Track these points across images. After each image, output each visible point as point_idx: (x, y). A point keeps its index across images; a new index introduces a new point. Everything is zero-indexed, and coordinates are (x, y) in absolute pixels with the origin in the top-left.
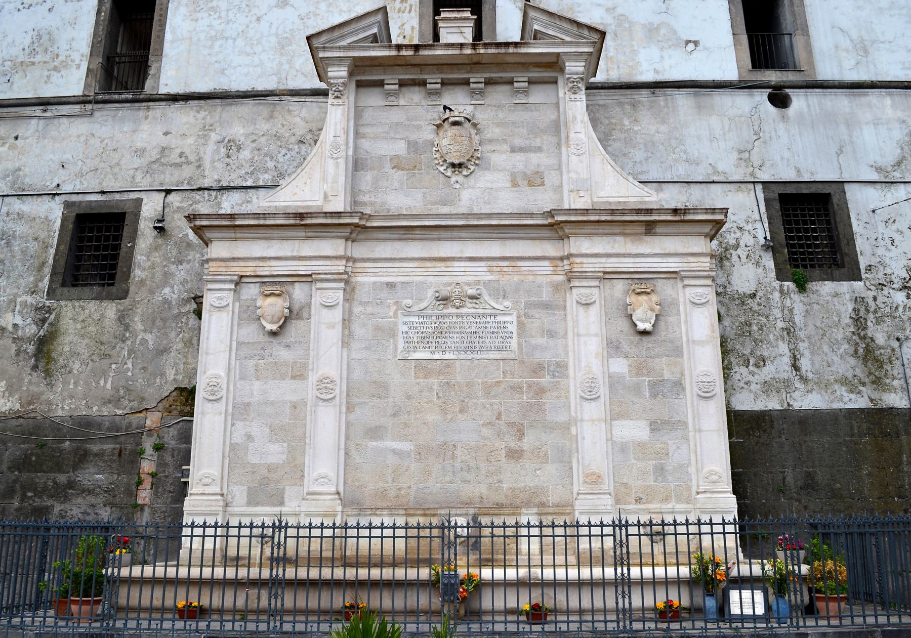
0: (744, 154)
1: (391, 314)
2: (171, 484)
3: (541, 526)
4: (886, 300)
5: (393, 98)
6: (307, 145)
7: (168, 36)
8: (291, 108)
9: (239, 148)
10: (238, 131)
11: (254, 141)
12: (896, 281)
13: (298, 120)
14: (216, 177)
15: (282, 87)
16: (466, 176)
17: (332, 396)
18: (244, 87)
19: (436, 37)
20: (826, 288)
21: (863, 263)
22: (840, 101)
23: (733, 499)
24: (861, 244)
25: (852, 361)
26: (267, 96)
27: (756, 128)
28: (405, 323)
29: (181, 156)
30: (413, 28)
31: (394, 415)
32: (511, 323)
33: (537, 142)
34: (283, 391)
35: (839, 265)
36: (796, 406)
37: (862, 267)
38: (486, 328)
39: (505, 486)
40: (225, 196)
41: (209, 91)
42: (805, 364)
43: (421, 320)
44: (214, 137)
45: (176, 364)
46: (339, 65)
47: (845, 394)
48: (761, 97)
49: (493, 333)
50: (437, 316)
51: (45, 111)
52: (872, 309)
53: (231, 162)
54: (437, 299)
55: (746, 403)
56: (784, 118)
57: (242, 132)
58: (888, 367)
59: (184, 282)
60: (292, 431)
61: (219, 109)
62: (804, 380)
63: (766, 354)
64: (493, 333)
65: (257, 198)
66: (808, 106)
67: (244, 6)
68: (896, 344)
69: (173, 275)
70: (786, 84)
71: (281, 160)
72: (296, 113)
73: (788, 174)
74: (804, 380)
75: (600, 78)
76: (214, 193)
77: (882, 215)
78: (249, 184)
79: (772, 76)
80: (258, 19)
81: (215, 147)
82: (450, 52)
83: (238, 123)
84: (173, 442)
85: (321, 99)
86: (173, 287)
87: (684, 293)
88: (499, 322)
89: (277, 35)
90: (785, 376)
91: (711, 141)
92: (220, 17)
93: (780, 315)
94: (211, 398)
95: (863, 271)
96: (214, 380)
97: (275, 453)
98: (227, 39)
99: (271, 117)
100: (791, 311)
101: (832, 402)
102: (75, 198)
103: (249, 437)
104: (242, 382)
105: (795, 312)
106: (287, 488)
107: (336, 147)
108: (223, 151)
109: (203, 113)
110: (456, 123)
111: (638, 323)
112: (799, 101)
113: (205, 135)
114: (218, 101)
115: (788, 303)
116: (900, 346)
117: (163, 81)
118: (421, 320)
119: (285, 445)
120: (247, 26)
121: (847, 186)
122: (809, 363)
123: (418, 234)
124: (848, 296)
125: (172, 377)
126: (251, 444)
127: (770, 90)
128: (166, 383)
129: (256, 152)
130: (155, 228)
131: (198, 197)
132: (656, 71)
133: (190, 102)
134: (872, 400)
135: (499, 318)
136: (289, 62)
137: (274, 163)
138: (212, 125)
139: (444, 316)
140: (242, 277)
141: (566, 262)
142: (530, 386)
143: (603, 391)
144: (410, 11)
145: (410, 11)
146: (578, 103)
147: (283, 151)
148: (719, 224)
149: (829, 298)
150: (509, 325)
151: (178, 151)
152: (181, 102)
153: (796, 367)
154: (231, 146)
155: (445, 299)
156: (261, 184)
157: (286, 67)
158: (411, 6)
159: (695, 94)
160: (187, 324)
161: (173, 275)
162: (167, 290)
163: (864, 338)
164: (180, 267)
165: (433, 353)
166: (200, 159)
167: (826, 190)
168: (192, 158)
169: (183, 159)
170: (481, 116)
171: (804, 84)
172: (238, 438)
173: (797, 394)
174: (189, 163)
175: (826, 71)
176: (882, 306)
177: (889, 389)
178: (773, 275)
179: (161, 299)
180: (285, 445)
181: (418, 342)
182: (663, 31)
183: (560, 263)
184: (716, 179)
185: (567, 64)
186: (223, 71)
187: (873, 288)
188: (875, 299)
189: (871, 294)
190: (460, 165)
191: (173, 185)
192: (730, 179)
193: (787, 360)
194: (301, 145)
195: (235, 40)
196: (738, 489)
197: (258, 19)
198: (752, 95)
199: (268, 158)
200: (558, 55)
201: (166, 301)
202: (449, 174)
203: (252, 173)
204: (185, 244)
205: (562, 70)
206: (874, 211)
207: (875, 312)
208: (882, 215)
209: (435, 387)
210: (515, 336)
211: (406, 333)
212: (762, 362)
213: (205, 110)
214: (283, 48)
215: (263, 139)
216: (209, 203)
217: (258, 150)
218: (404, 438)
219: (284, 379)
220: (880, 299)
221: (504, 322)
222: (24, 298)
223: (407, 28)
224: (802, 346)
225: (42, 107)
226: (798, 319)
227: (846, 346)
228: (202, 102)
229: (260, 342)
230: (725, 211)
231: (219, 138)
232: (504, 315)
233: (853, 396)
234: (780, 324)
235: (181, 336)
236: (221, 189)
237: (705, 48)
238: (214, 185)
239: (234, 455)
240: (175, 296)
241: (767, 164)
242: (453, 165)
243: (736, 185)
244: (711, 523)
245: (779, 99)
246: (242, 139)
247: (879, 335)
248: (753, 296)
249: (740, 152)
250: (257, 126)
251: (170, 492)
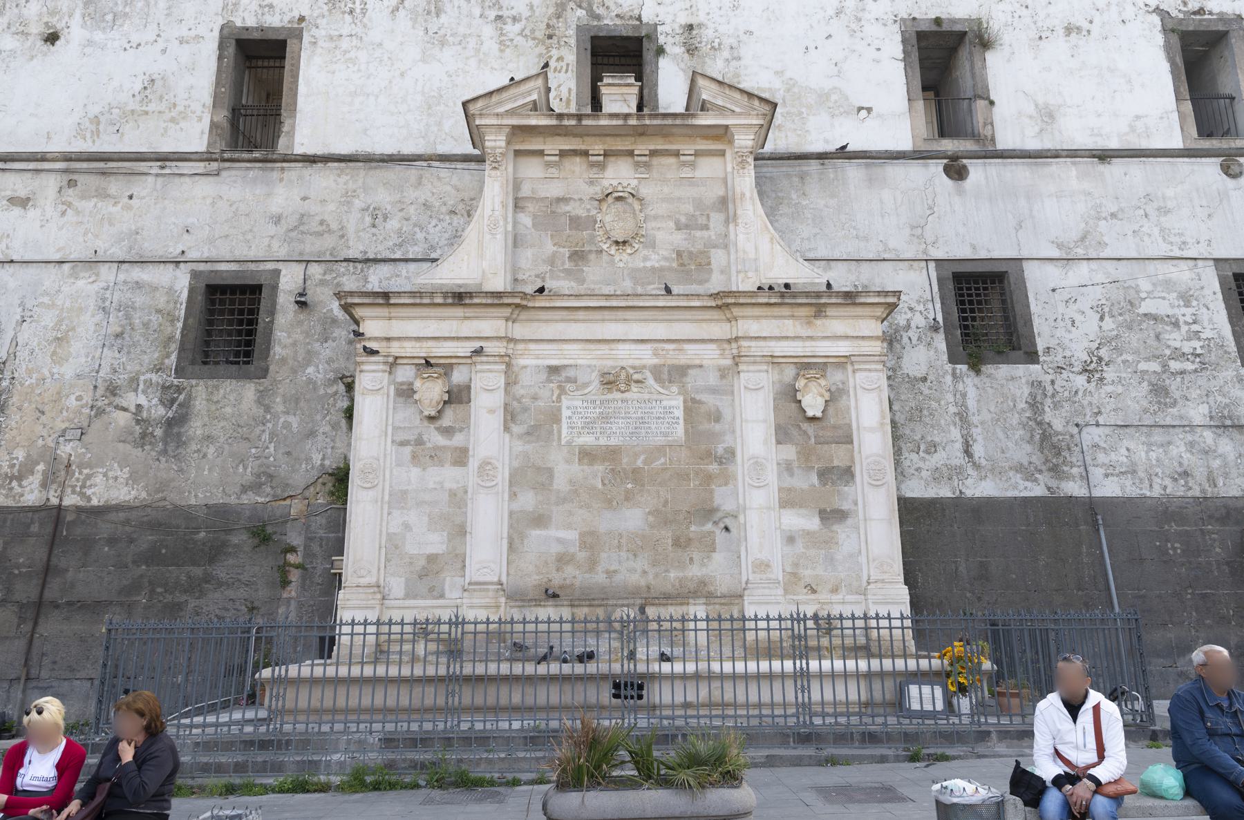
0: (917, 230)
3: (708, 620)
4: (1065, 383)
5: (553, 170)
7: (302, 89)
8: (442, 175)
9: (385, 218)
10: (383, 198)
14: (361, 248)
18: (389, 149)
19: (596, 104)
20: (1003, 371)
21: (1041, 345)
22: (1018, 172)
23: (904, 592)
25: (1028, 448)
27: (930, 202)
29: (322, 223)
30: (570, 90)
32: (677, 408)
36: (969, 493)
40: (371, 270)
42: (978, 450)
44: (358, 204)
48: (937, 167)
50: (602, 402)
51: (162, 168)
52: (1049, 394)
55: (917, 489)
56: (960, 193)
59: (329, 361)
61: (362, 173)
62: (977, 466)
63: (937, 439)
66: (986, 178)
67: (385, 58)
68: (1076, 430)
71: (432, 231)
74: (977, 466)
75: (769, 148)
76: (359, 266)
78: (397, 256)
79: (948, 145)
80: (402, 75)
82: (614, 122)
83: (379, 189)
85: (473, 165)
90: (957, 462)
91: (883, 216)
92: (359, 70)
93: (952, 400)
97: (436, 543)
100: (964, 395)
101: (1006, 490)
102: (202, 267)
103: (407, 527)
108: (368, 220)
109: (344, 178)
110: (619, 199)
112: (977, 171)
115: (960, 387)
117: (298, 138)
121: (1025, 264)
122: (982, 450)
124: (1023, 380)
127: (945, 161)
130: (297, 302)
132: (826, 141)
134: (1049, 489)
136: (439, 124)
140: (397, 358)
141: (734, 345)
142: (697, 474)
144: (567, 71)
145: (567, 71)
147: (434, 222)
148: (892, 307)
149: (1004, 382)
151: (318, 218)
152: (320, 165)
153: (968, 452)
154: (377, 216)
157: (435, 129)
159: (867, 165)
160: (334, 405)
162: (310, 370)
163: (1040, 424)
164: (325, 345)
168: (334, 226)
170: (644, 191)
172: (395, 527)
173: (969, 482)
175: (1005, 140)
176: (1058, 389)
177: (1069, 477)
178: (945, 357)
182: (834, 97)
184: (887, 256)
186: (365, 131)
187: (1050, 371)
188: (1053, 382)
190: (624, 242)
192: (902, 257)
193: (959, 445)
195: (377, 97)
196: (909, 580)
197: (402, 75)
198: (926, 165)
199: (417, 229)
200: (727, 127)
201: (310, 381)
202: (612, 252)
203: (401, 245)
205: (731, 142)
206: (1054, 290)
207: (1053, 396)
210: (681, 421)
212: (933, 448)
214: (430, 108)
215: (412, 210)
217: (407, 220)
218: (569, 527)
220: (1059, 383)
222: (148, 376)
224: (975, 432)
225: (159, 163)
226: (971, 403)
227: (1021, 432)
228: (343, 165)
230: (897, 294)
231: (363, 205)
233: (1028, 484)
234: (952, 409)
236: (367, 261)
238: (360, 256)
239: (392, 546)
242: (617, 243)
244: (889, 618)
245: (956, 171)
246: (389, 207)
247: (1057, 421)
248: (924, 379)
249: (913, 228)
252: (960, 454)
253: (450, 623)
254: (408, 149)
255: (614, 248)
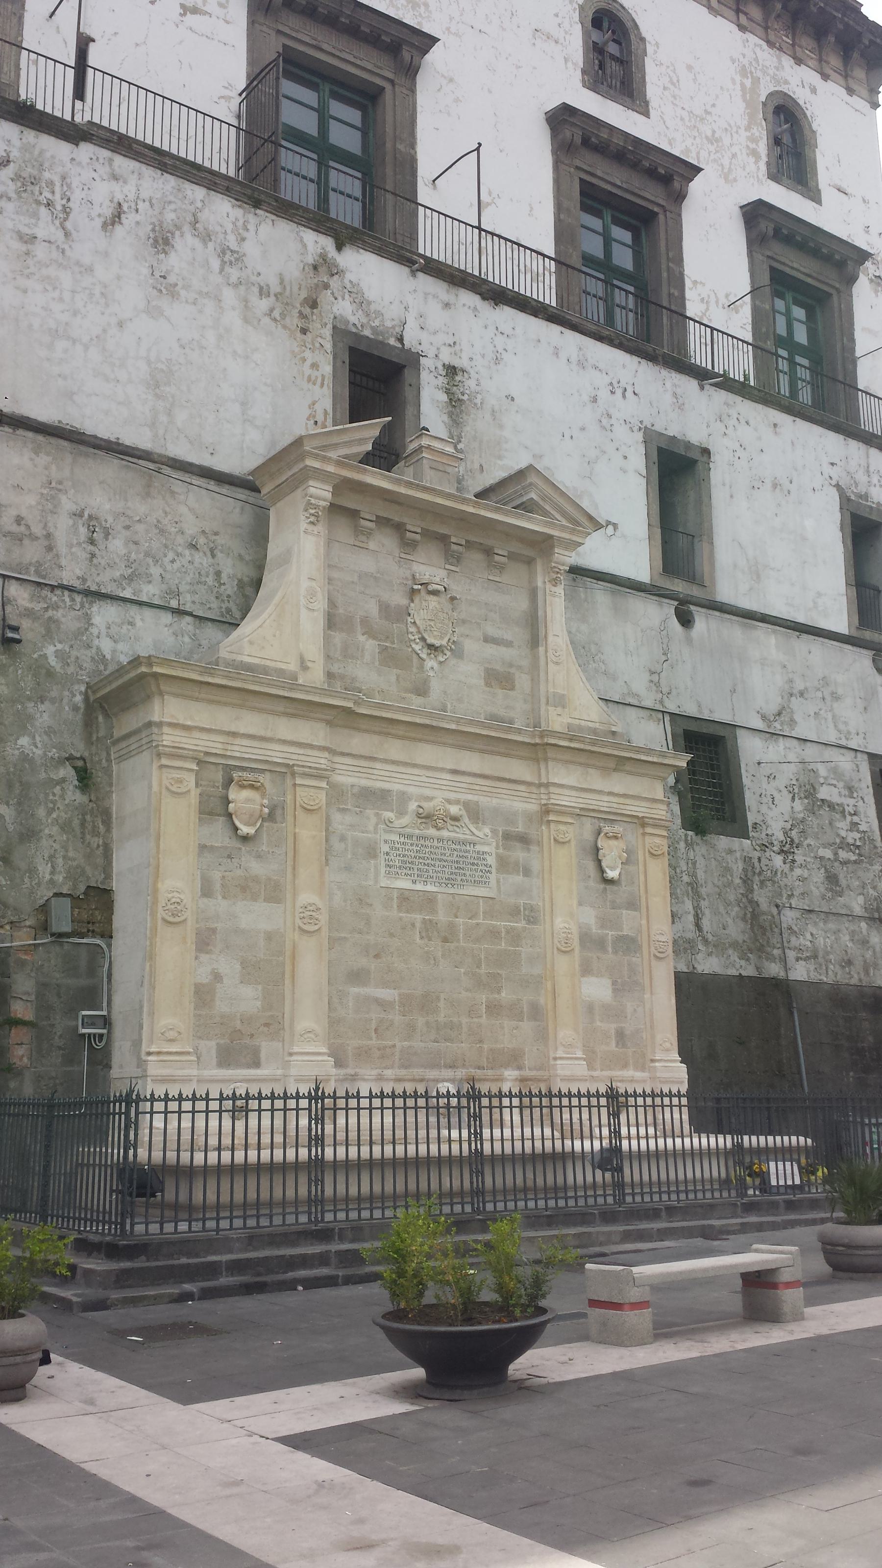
1: (371, 828)
2: (61, 1036)
4: (768, 862)
5: (364, 538)
6: (201, 554)
8: (174, 488)
9: (107, 535)
10: (101, 503)
11: (127, 528)
12: (775, 843)
13: (183, 509)
14: (79, 573)
15: (159, 450)
16: (441, 663)
17: (316, 927)
18: (104, 432)
20: (723, 842)
21: (751, 818)
22: (733, 631)
24: (750, 800)
25: (741, 925)
26: (139, 458)
27: (665, 646)
28: (386, 842)
29: (19, 520)
31: (377, 956)
32: (490, 854)
33: (508, 636)
34: (254, 917)
35: (733, 820)
36: (700, 969)
37: (750, 824)
38: (466, 857)
39: (485, 1046)
40: (95, 608)
41: (50, 422)
42: (706, 923)
43: (402, 840)
44: (67, 504)
45: (52, 857)
46: (323, 481)
47: (737, 960)
48: (669, 609)
49: (473, 864)
50: (419, 838)
52: (757, 871)
53: (97, 551)
54: (419, 816)
57: (107, 506)
58: (768, 934)
59: (49, 731)
60: (270, 969)
61: (69, 458)
62: (706, 941)
64: (473, 864)
65: (142, 620)
66: (708, 630)
67: (97, 291)
68: (775, 911)
69: (30, 718)
70: (694, 599)
71: (169, 567)
72: (182, 497)
73: (691, 710)
74: (706, 941)
76: (78, 598)
77: (766, 770)
78: (127, 594)
79: (679, 586)
80: (121, 325)
81: (71, 522)
83: (101, 490)
84: (58, 975)
86: (34, 738)
87: (644, 841)
88: (478, 852)
89: (149, 363)
90: (690, 935)
91: (626, 654)
92: (61, 300)
93: (685, 868)
94: (171, 919)
95: (750, 828)
96: (175, 894)
98: (74, 342)
99: (148, 494)
100: (694, 864)
101: (727, 967)
103: (217, 977)
104: (205, 900)
105: (698, 865)
106: (264, 1044)
107: (312, 594)
108: (83, 531)
109: (43, 459)
111: (608, 870)
112: (702, 622)
113: (53, 497)
114: (65, 443)
115: (691, 855)
116: (779, 914)
118: (402, 840)
119: (260, 987)
120: (104, 331)
122: (708, 923)
123: (401, 730)
124: (738, 855)
125: (48, 877)
126: (218, 985)
127: (676, 603)
128: (39, 884)
129: (133, 547)
131: (55, 599)
133: (20, 432)
134: (757, 968)
135: (478, 848)
136: (169, 413)
137: (160, 571)
138: (60, 483)
139: (425, 838)
141: (543, 790)
142: (508, 932)
143: (576, 944)
144: (322, 385)
145: (322, 385)
146: (557, 599)
147: (171, 555)
149: (723, 854)
150: (487, 857)
151: (13, 512)
153: (698, 926)
154: (95, 530)
155: (428, 817)
156: (145, 599)
157: (163, 418)
158: (323, 377)
159: (613, 592)
160: (62, 797)
161: (30, 718)
162: (24, 741)
163: (751, 901)
164: (42, 708)
165: (414, 882)
166: (48, 536)
167: (721, 732)
168: (37, 530)
169: (22, 528)
171: (707, 603)
173: (700, 957)
174: (33, 538)
175: (725, 593)
176: (765, 868)
177: (771, 958)
178: (679, 821)
179: (16, 752)
180: (260, 987)
181: (400, 867)
183: (535, 790)
185: (556, 550)
187: (758, 848)
188: (759, 859)
189: (756, 854)
191: (11, 569)
192: (643, 704)
193: (691, 918)
194: (193, 551)
195: (86, 348)
197: (121, 325)
199: (150, 561)
200: (551, 537)
201: (25, 758)
202: (424, 656)
204: (44, 671)
206: (759, 763)
207: (760, 874)
208: (766, 770)
209: (418, 925)
210: (494, 870)
211: (387, 854)
213: (48, 454)
214: (157, 386)
215: (140, 528)
216: (73, 613)
217: (136, 543)
218: (385, 985)
219: (255, 900)
220: (764, 861)
221: (483, 853)
223: (319, 408)
224: (704, 904)
226: (700, 874)
227: (736, 909)
228: (40, 438)
229: (226, 848)
231: (74, 508)
232: (483, 844)
233: (743, 963)
234: (686, 879)
235: (54, 815)
237: (624, 536)
240: (39, 752)
241: (674, 692)
242: (431, 647)
243: (648, 713)
246: (110, 520)
250: (129, 504)
251: (60, 1048)
252: (692, 927)
253: (310, 1097)
254: (129, 439)
255: (425, 650)
